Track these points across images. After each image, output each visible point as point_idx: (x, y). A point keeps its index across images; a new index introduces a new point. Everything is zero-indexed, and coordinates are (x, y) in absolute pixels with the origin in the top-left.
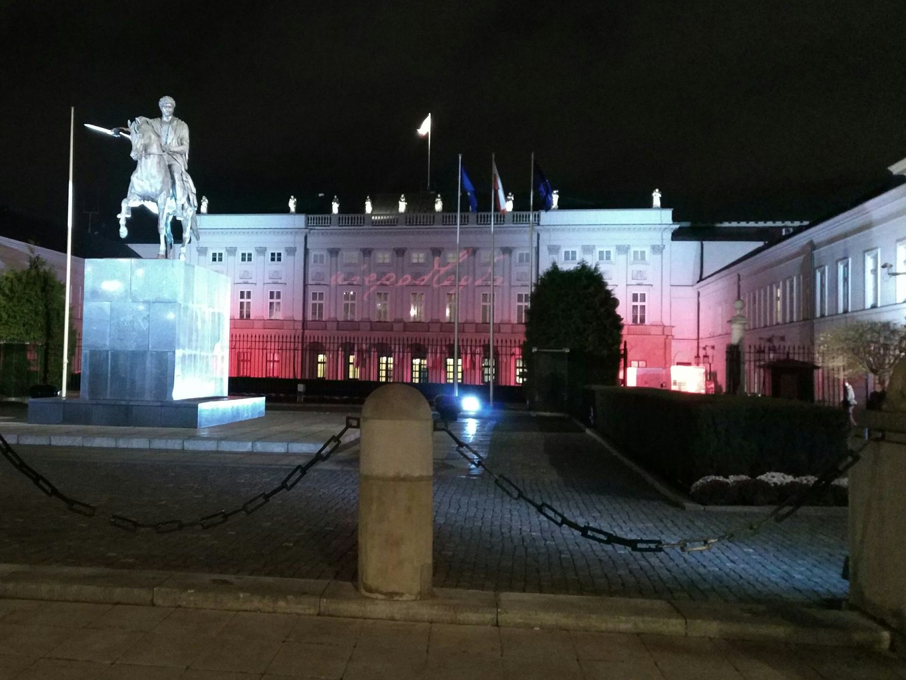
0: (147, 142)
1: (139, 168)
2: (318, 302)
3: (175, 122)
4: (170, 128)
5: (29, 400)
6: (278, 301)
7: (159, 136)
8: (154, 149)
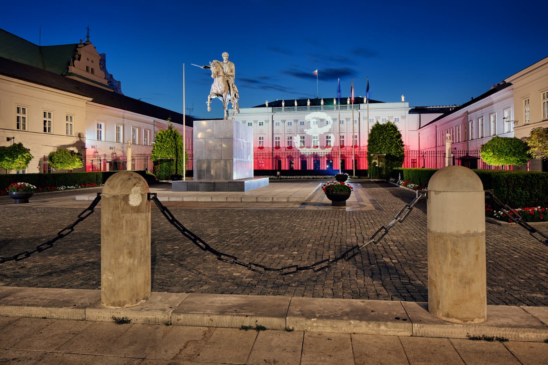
0: (218, 71)
1: (214, 82)
2: (278, 140)
3: (229, 63)
4: (227, 66)
5: (170, 181)
6: (263, 140)
7: (223, 68)
8: (221, 74)
